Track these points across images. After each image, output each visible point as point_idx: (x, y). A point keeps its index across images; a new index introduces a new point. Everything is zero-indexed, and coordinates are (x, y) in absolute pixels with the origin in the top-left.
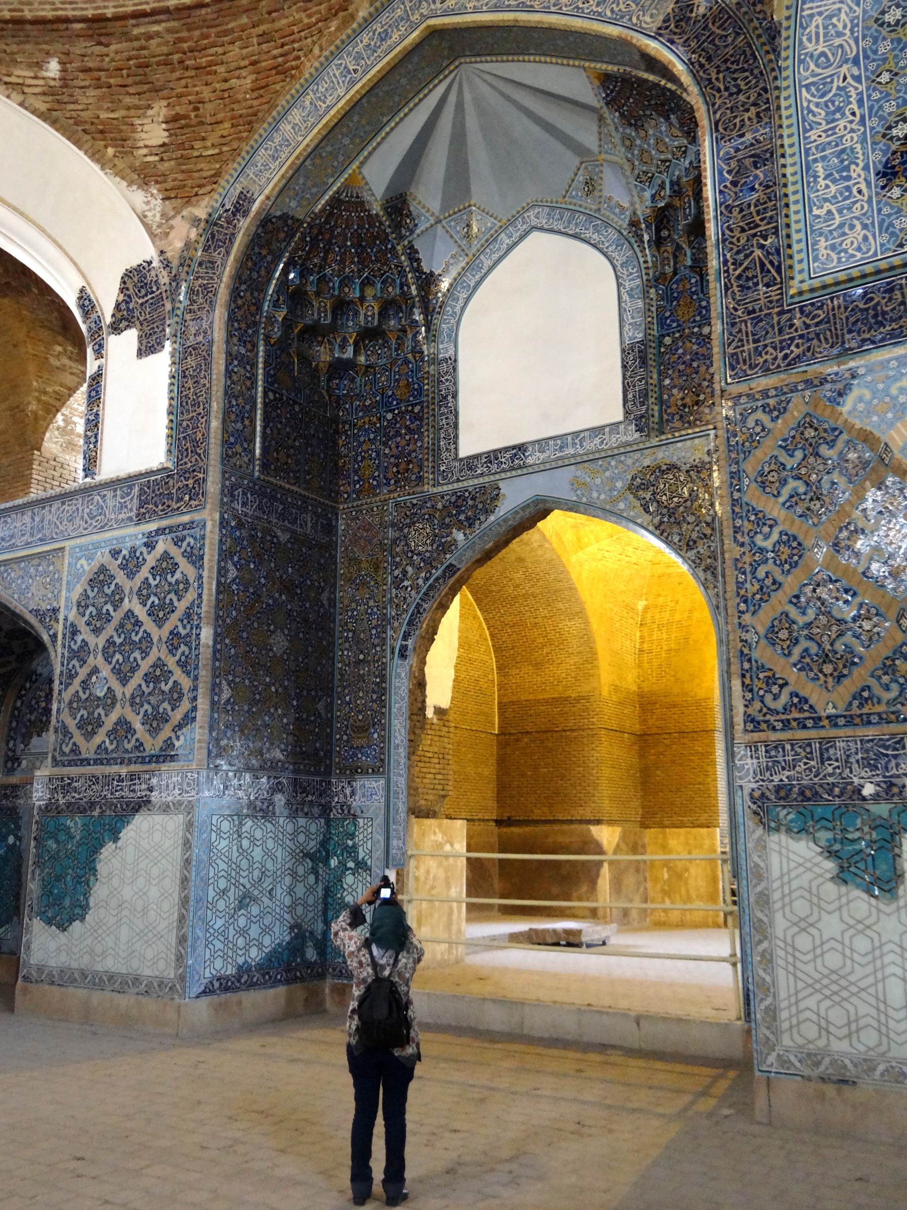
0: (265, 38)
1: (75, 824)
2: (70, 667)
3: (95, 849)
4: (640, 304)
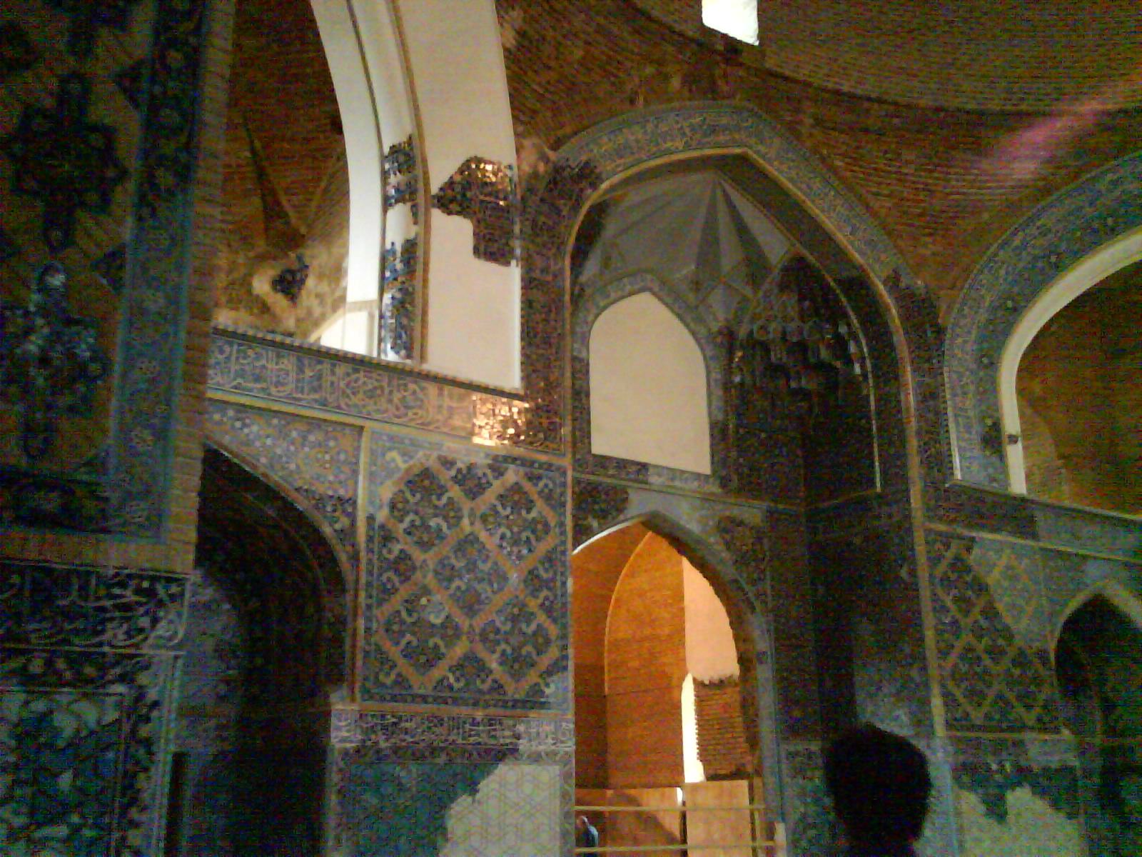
0: (600, 30)
1: (409, 774)
2: (384, 578)
3: (440, 804)
4: (720, 393)
